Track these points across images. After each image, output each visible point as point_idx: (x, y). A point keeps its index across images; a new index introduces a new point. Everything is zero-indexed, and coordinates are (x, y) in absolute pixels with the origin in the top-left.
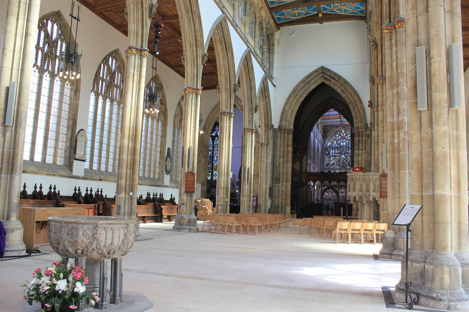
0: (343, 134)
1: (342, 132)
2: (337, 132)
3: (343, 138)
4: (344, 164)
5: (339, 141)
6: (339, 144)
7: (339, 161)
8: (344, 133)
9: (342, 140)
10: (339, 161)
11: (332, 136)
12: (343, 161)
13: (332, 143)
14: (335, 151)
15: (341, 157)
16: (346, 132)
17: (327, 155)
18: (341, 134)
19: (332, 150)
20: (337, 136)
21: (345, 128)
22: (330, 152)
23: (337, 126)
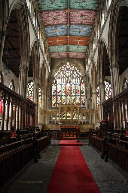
0: (68, 66)
1: (67, 65)
2: (62, 64)
3: (68, 69)
4: (69, 91)
5: (65, 72)
6: (65, 74)
7: (65, 88)
8: (69, 65)
9: (67, 71)
10: (65, 88)
11: (59, 68)
12: (68, 89)
13: (59, 73)
14: (61, 80)
15: (67, 86)
16: (71, 64)
17: (54, 83)
18: (67, 66)
19: (59, 79)
20: (63, 67)
21: (70, 61)
22: (57, 81)
23: (62, 59)
